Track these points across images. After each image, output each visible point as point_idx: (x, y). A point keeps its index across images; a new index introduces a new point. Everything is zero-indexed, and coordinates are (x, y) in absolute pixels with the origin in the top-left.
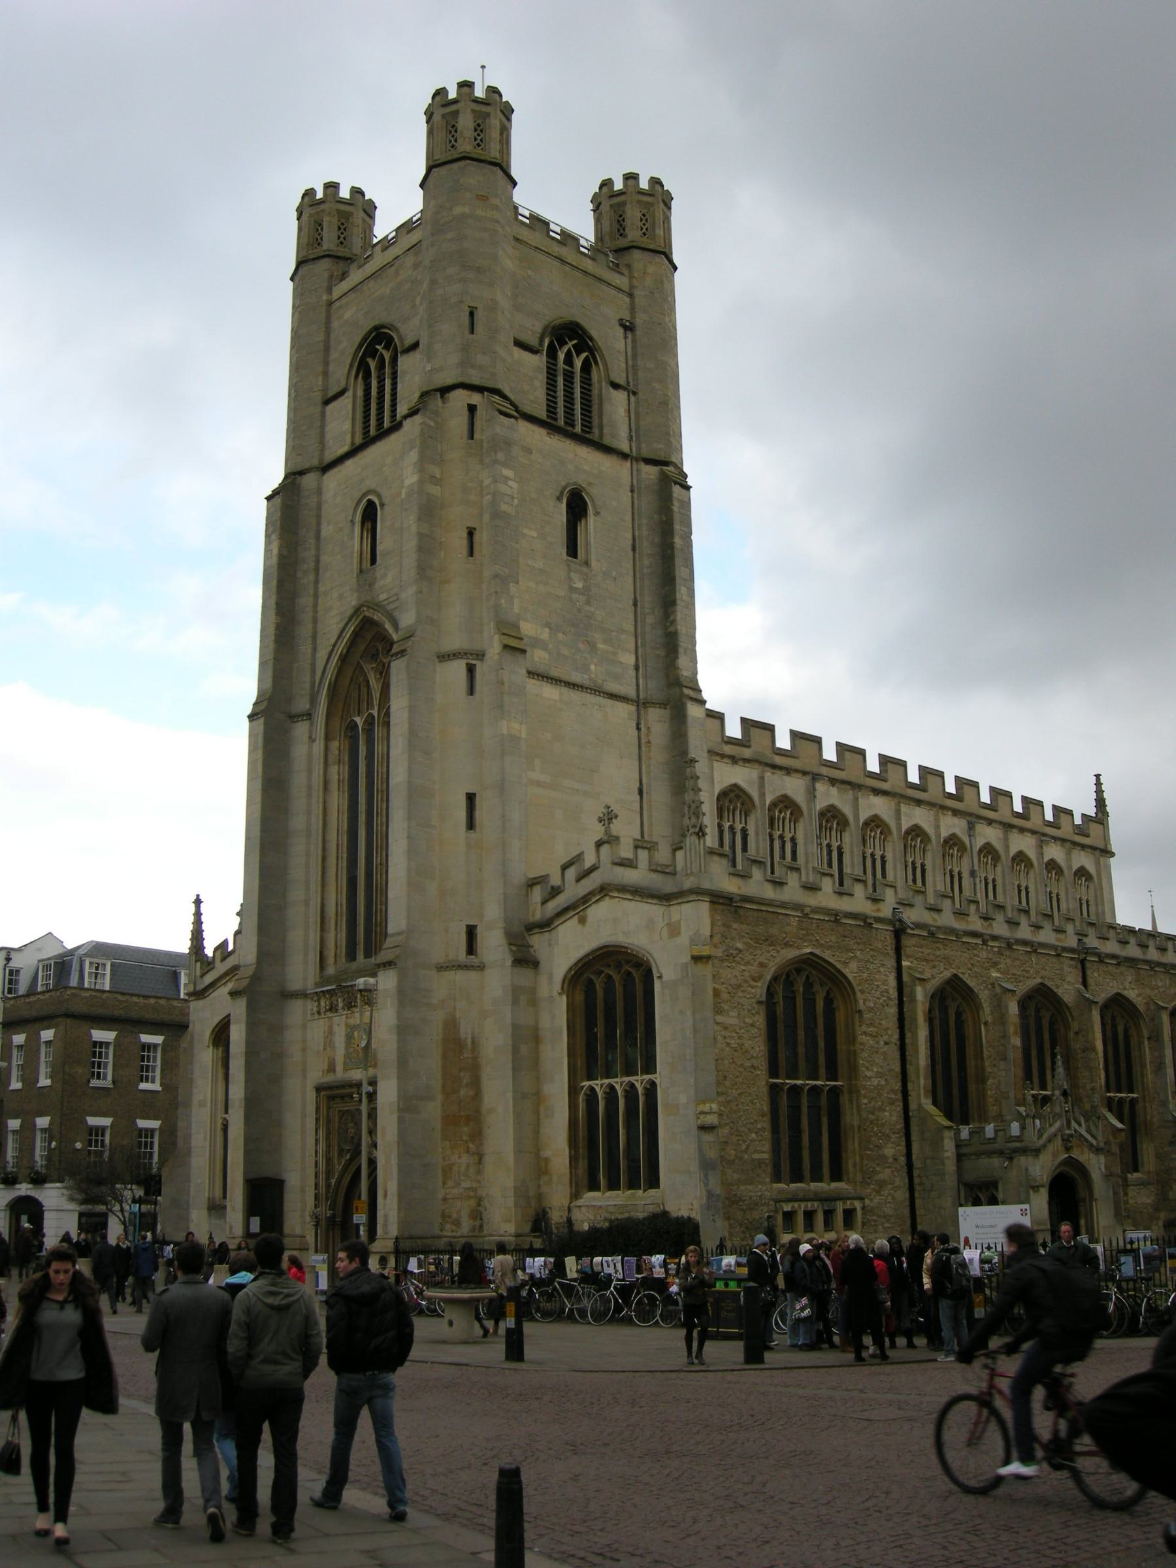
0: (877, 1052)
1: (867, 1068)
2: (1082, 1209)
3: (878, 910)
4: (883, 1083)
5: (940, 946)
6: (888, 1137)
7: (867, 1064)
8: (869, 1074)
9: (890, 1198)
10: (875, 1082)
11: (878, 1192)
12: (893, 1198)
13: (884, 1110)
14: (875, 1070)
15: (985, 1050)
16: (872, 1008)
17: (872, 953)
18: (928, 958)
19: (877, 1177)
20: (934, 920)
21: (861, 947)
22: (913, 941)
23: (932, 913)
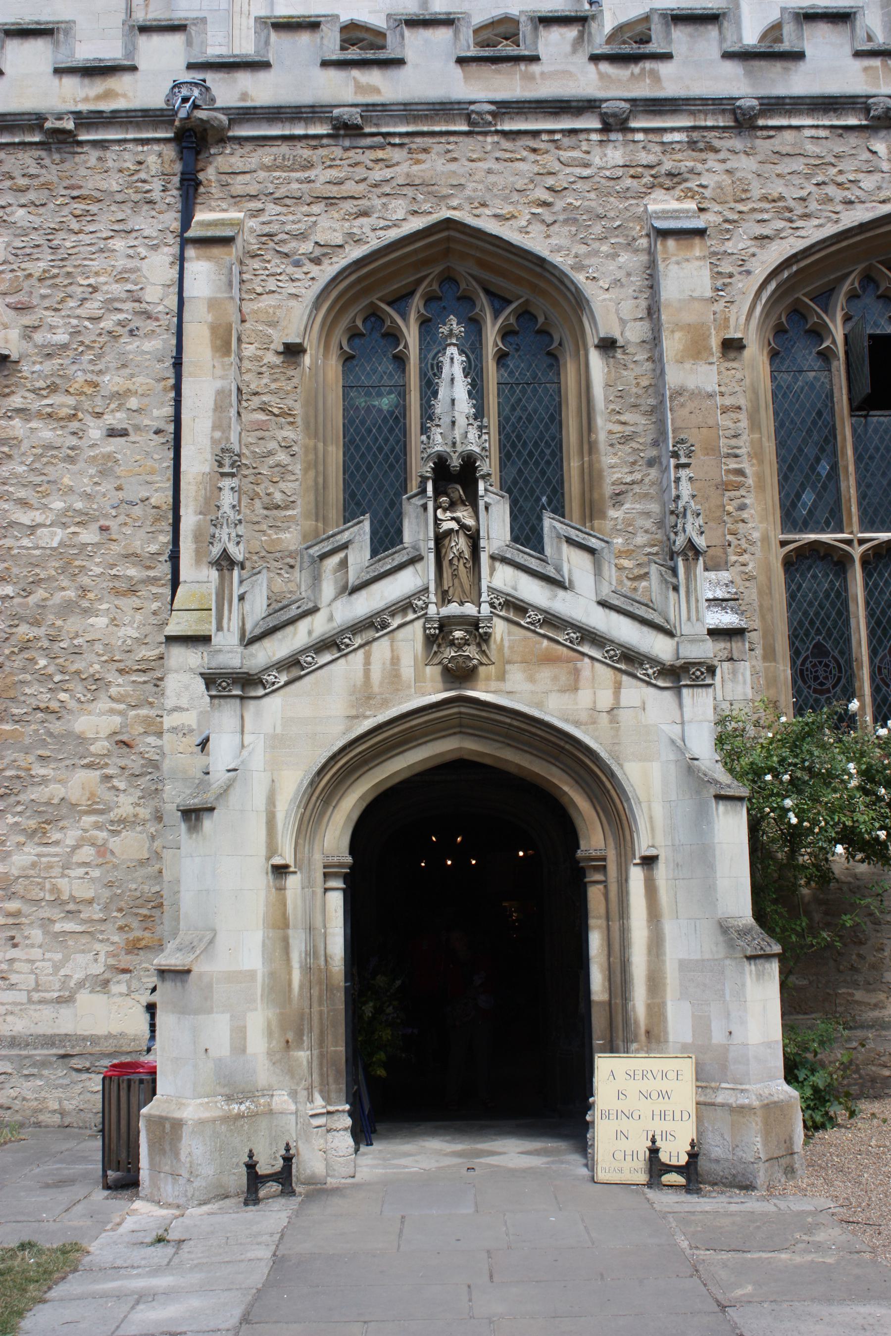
0: (71, 460)
1: (24, 503)
2: (594, 894)
3: (108, 95)
4: (89, 536)
5: (397, 155)
6: (98, 683)
7: (22, 493)
8: (25, 518)
9: (87, 853)
10: (54, 537)
11: (37, 834)
12: (102, 850)
13: (87, 612)
14: (58, 505)
15: (600, 421)
16: (65, 347)
17: (79, 207)
18: (334, 191)
19: (35, 794)
20: (359, 88)
21: (32, 195)
22: (267, 155)
23: (355, 73)
